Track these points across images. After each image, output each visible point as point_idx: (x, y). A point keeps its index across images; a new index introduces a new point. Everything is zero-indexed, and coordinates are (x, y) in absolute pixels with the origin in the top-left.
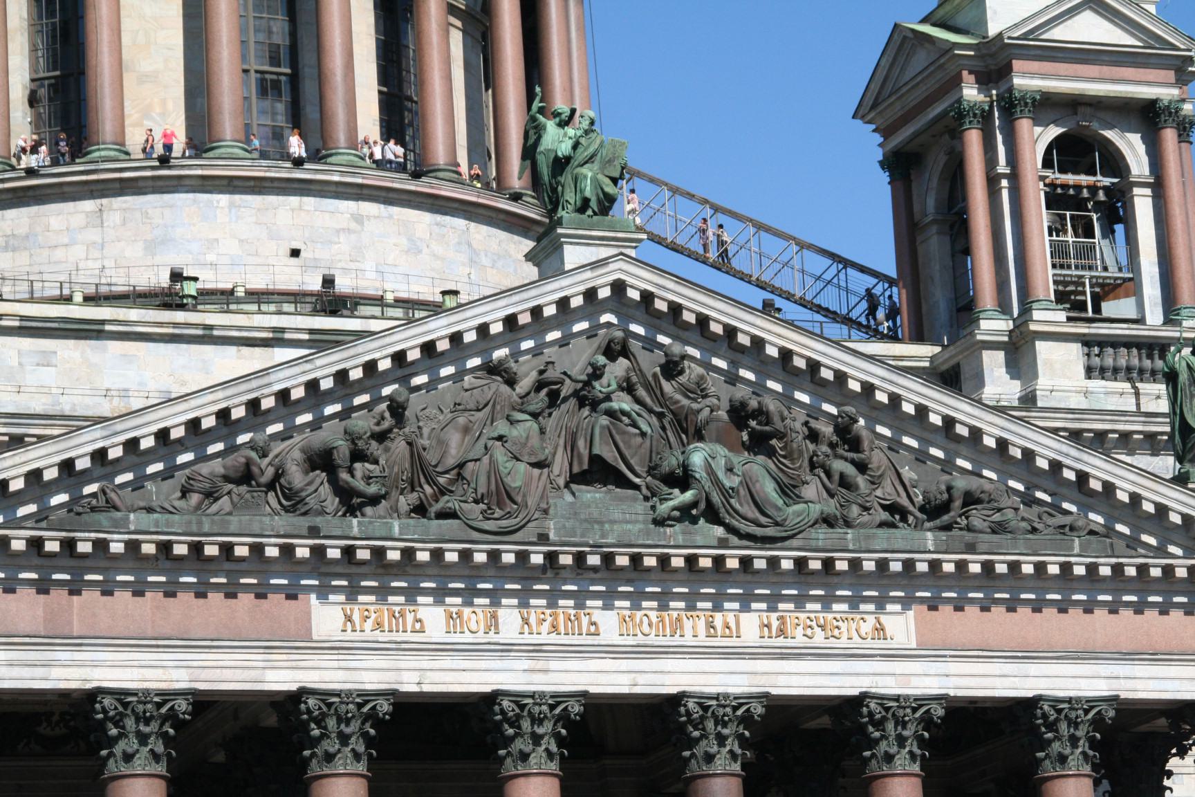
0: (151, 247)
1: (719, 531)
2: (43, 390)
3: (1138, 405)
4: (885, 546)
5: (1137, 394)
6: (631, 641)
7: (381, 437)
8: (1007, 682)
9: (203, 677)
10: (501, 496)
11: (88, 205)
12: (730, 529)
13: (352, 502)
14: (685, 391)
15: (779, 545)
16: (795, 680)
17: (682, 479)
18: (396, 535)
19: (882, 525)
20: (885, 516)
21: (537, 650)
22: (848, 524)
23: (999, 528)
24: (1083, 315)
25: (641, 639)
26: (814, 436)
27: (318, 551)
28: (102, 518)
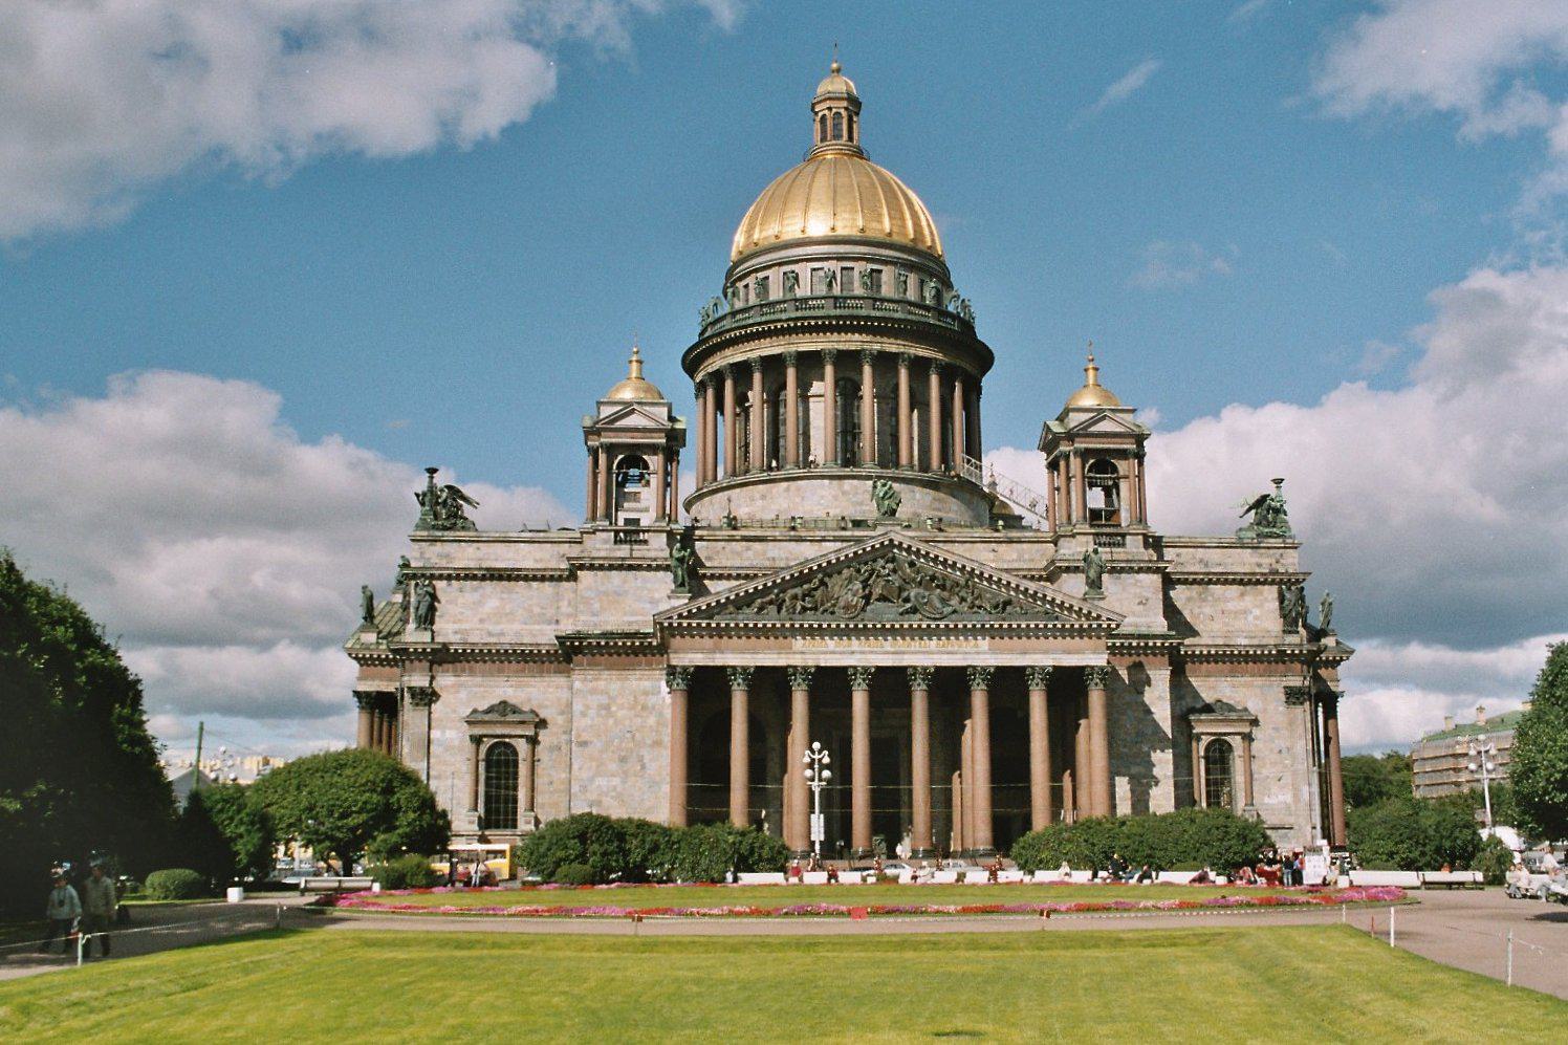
0: (803, 498)
2: (748, 559)
6: (893, 650)
7: (816, 589)
10: (847, 607)
11: (784, 485)
12: (924, 616)
13: (804, 609)
17: (907, 600)
19: (975, 612)
20: (975, 609)
24: (1099, 522)
25: (897, 649)
26: (958, 584)
27: (792, 625)
28: (729, 617)
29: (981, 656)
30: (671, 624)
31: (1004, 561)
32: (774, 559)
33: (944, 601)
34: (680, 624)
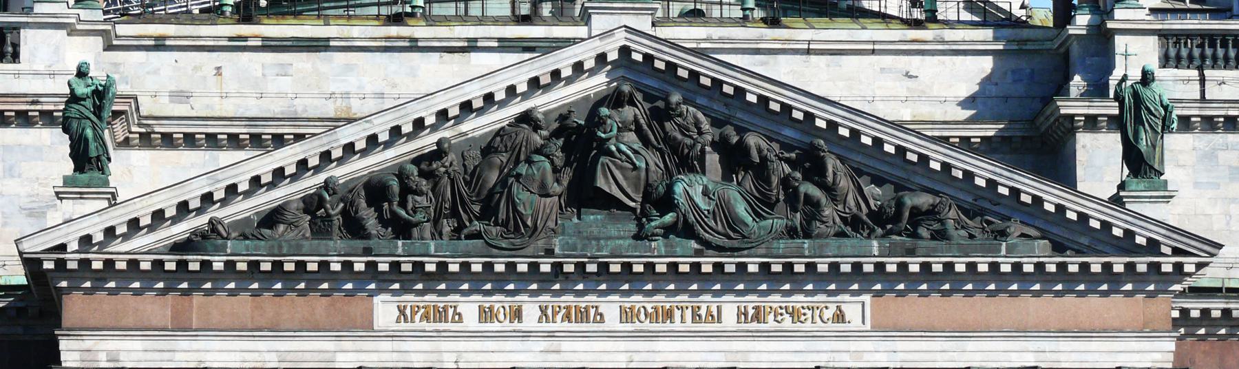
1: (694, 244)
2: (281, 95)
3: (1203, 92)
4: (836, 252)
5: (1202, 81)
8: (946, 356)
9: (289, 358)
13: (403, 229)
14: (683, 129)
15: (745, 252)
16: (765, 357)
18: (433, 252)
21: (551, 335)
22: (807, 235)
23: (940, 235)
25: (638, 326)
27: (371, 266)
29: (853, 345)
30: (61, 264)
31: (932, 100)
32: (346, 96)
33: (762, 204)
34: (85, 264)
